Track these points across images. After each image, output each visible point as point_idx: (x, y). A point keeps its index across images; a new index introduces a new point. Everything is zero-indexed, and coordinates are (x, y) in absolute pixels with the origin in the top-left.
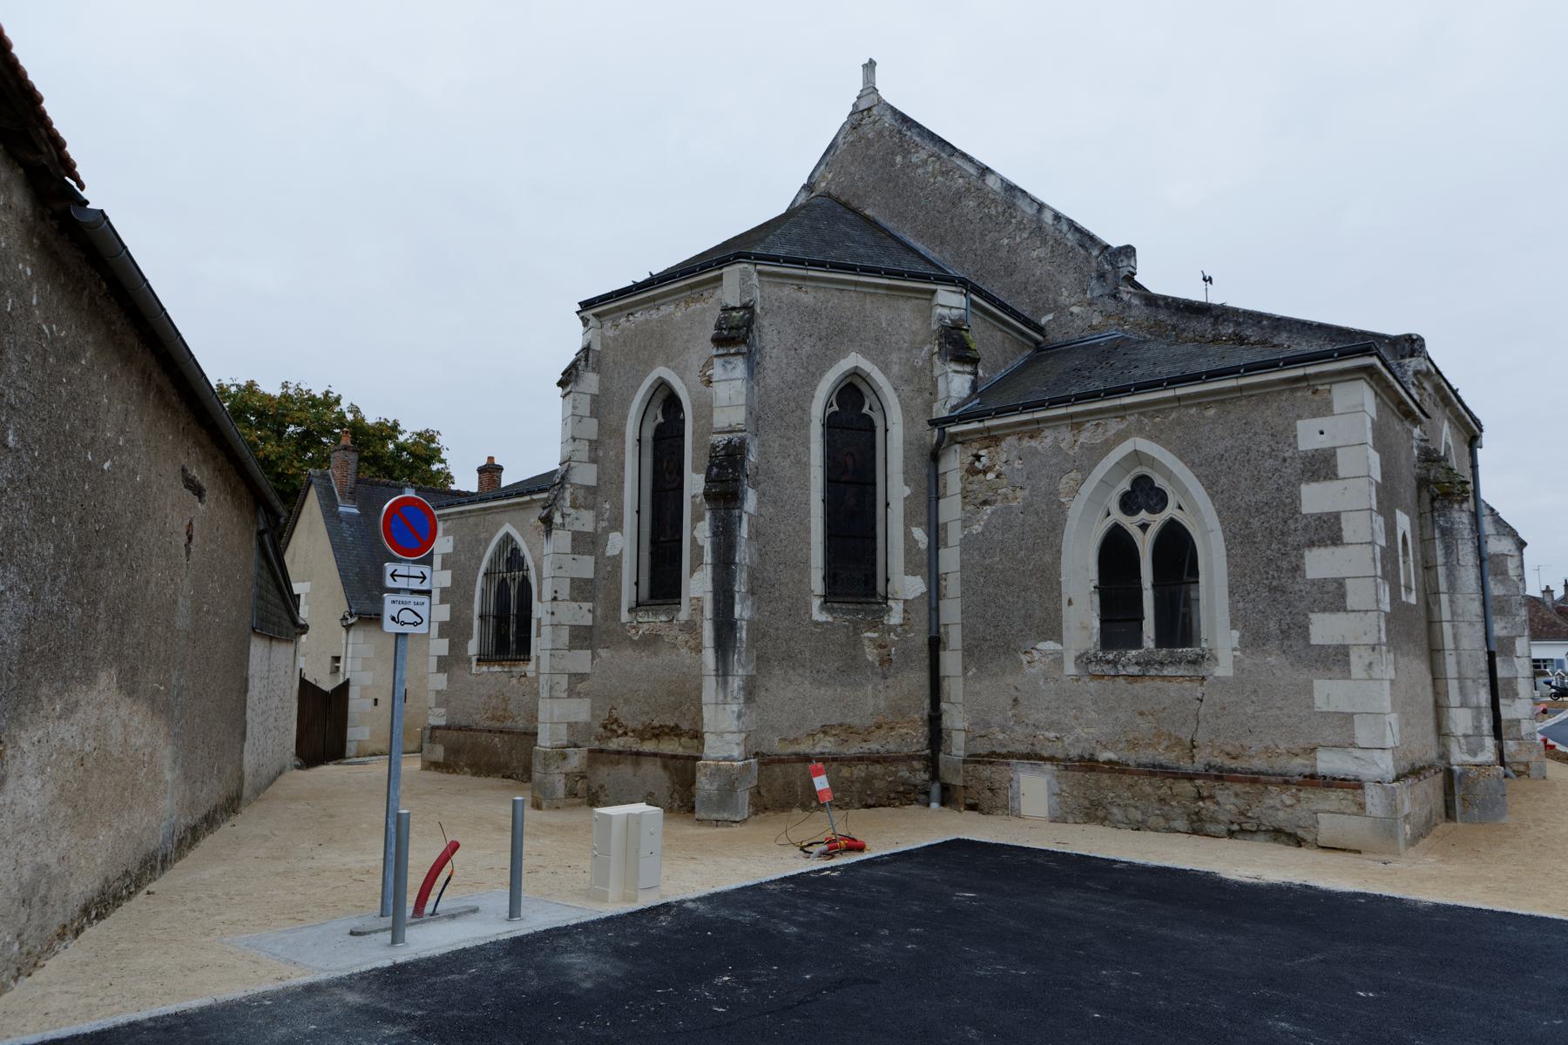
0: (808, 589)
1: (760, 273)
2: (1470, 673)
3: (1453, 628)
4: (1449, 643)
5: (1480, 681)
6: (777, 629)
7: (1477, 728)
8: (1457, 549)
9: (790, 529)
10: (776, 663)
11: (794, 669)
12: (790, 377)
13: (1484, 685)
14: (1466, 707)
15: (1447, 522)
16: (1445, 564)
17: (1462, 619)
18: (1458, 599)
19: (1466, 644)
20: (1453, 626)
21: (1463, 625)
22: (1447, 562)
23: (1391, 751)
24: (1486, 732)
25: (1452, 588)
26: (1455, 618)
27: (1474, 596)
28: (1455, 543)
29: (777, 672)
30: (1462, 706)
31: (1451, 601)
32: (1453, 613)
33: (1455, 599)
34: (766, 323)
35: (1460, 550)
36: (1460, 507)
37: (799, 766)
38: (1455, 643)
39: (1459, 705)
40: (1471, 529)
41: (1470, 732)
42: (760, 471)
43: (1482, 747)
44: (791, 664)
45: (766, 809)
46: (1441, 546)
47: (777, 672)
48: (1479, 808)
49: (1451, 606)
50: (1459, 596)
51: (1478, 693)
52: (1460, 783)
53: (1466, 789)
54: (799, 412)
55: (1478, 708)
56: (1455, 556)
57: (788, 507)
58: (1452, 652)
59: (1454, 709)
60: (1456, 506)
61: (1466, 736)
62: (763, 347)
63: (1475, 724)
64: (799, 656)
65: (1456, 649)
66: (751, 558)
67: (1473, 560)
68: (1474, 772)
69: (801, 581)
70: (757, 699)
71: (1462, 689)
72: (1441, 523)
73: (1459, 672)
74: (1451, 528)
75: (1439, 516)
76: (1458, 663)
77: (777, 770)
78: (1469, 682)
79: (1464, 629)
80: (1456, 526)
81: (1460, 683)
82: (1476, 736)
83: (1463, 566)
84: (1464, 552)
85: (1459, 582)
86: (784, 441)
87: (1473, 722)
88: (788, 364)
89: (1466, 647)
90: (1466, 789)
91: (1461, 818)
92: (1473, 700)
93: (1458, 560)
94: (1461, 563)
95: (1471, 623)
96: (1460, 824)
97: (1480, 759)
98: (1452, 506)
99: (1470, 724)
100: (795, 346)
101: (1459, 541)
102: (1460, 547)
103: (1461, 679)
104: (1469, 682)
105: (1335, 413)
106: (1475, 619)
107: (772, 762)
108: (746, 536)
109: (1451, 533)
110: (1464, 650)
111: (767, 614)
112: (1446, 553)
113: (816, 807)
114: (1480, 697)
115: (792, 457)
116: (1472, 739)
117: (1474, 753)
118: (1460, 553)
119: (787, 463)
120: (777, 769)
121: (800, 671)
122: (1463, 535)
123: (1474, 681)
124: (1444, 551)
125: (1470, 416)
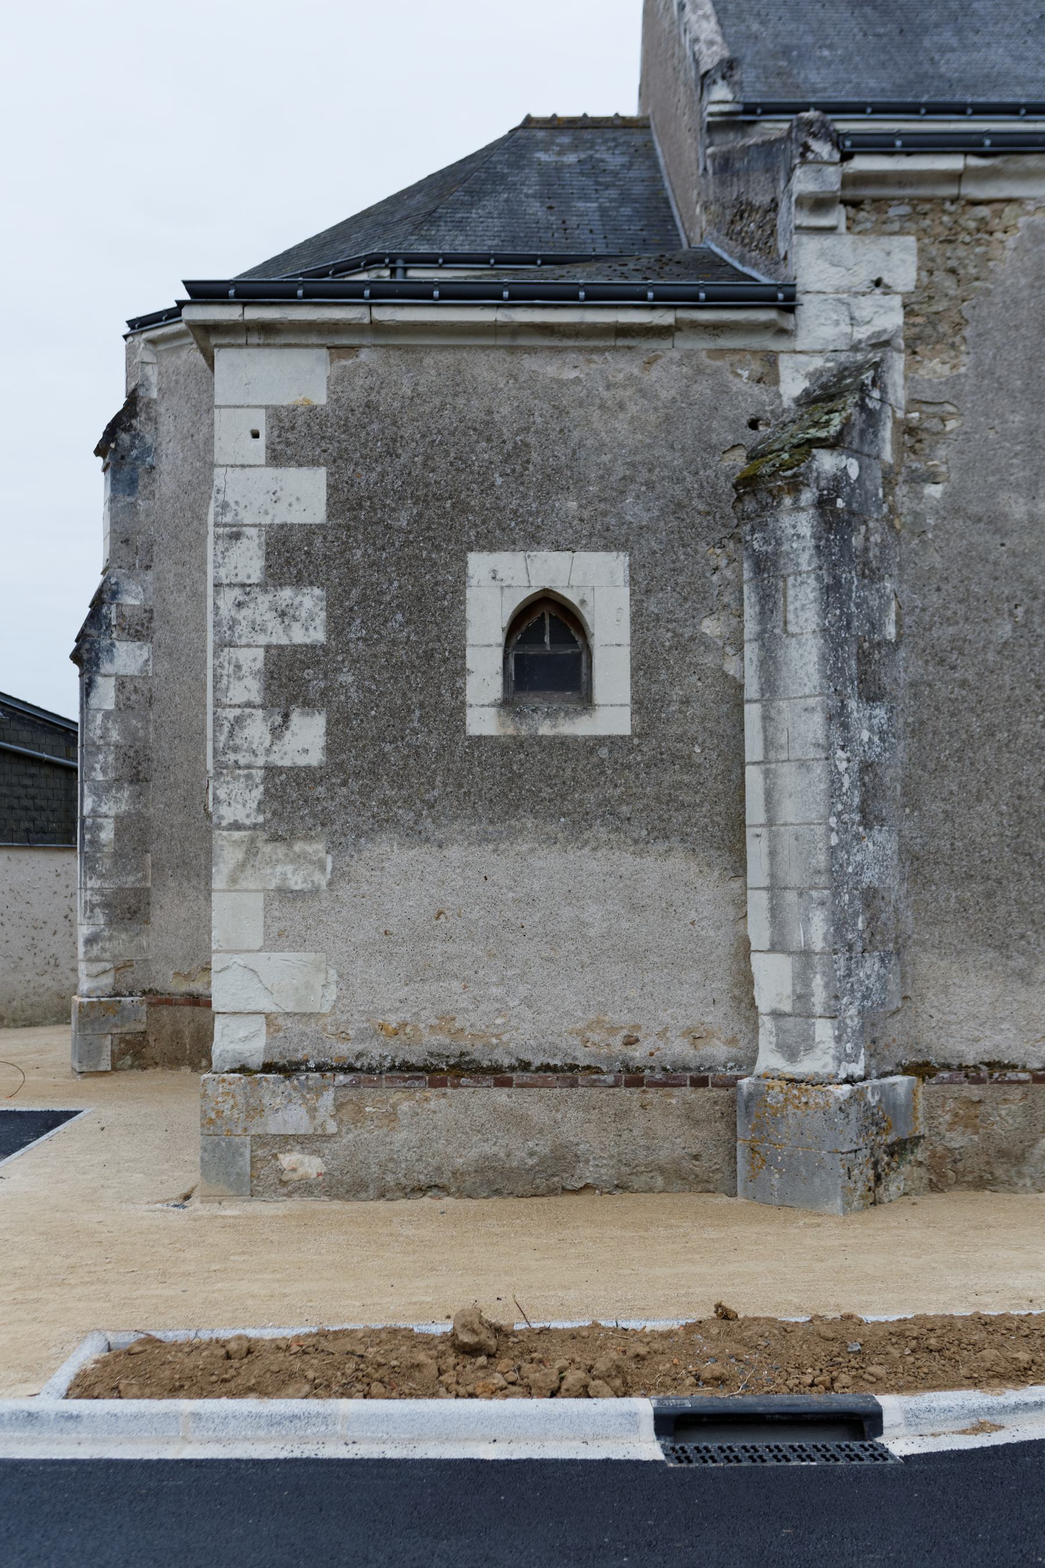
0: (203, 769)
1: (152, 342)
2: (793, 876)
3: (766, 778)
4: (755, 811)
5: (814, 894)
6: (172, 826)
7: (802, 998)
8: (785, 597)
9: (185, 688)
10: (170, 873)
11: (189, 881)
12: (186, 478)
13: (823, 904)
14: (782, 951)
15: (766, 541)
16: (760, 637)
17: (784, 756)
18: (779, 712)
19: (789, 811)
20: (767, 774)
21: (785, 769)
22: (764, 631)
23: (261, 1019)
24: (818, 1009)
25: (770, 687)
26: (772, 755)
27: (812, 702)
28: (781, 584)
29: (171, 883)
30: (773, 949)
31: (766, 718)
32: (769, 744)
33: (773, 713)
34: (162, 410)
35: (790, 599)
36: (796, 500)
37: (187, 1010)
38: (768, 810)
39: (767, 946)
40: (817, 547)
41: (787, 1007)
42: (155, 615)
43: (808, 1043)
44: (185, 873)
45: (157, 1064)
46: (754, 599)
47: (171, 883)
48: (780, 1171)
49: (765, 729)
50: (783, 704)
51: (807, 920)
52: (748, 1114)
53: (759, 1128)
54: (196, 523)
55: (806, 953)
56: (780, 617)
57: (183, 659)
58: (758, 831)
59: (758, 955)
60: (788, 501)
61: (777, 1015)
62: (160, 444)
63: (798, 991)
64: (194, 862)
65: (770, 822)
66: (126, 731)
67: (816, 619)
68: (775, 1096)
69: (196, 759)
70: (152, 919)
71: (775, 911)
72: (756, 546)
73: (772, 876)
74: (775, 554)
75: (753, 531)
76: (772, 854)
77: (165, 1013)
78: (791, 897)
79: (789, 778)
80: (785, 547)
81: (771, 899)
82: (799, 1015)
83: (793, 635)
84: (798, 604)
85: (784, 673)
86: (180, 569)
87: (794, 985)
88: (184, 460)
89: (791, 819)
90: (759, 1128)
91: (745, 1189)
92: (797, 938)
93: (785, 623)
94: (792, 628)
95: (803, 764)
96: (740, 1200)
97: (807, 1066)
98: (779, 503)
99: (788, 990)
100: (192, 431)
101: (791, 580)
102: (791, 593)
103: (775, 888)
104: (791, 897)
105: (263, 411)
106: (812, 753)
107: (160, 1003)
108: (110, 705)
109: (775, 564)
110: (785, 824)
111: (162, 806)
112: (762, 613)
113: (205, 1067)
114: (813, 930)
115: (188, 588)
116: (789, 1023)
117: (792, 1054)
118: (791, 608)
119: (182, 599)
120: (165, 1012)
121: (194, 882)
122: (798, 564)
123: (800, 895)
124: (757, 609)
125: (471, 347)
